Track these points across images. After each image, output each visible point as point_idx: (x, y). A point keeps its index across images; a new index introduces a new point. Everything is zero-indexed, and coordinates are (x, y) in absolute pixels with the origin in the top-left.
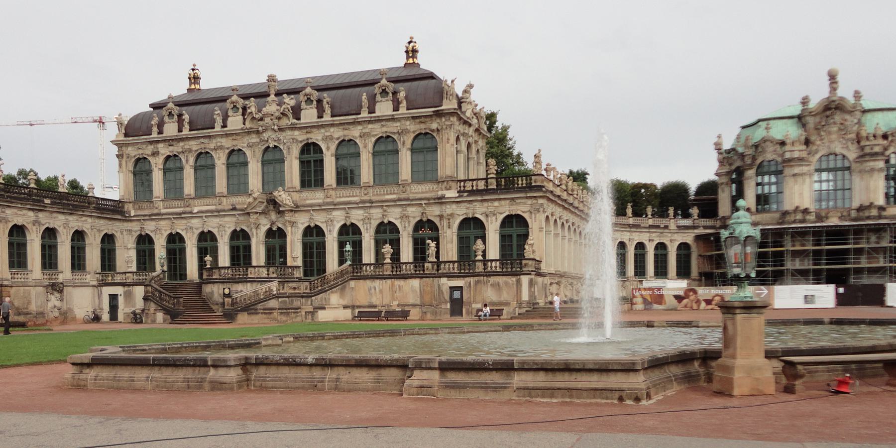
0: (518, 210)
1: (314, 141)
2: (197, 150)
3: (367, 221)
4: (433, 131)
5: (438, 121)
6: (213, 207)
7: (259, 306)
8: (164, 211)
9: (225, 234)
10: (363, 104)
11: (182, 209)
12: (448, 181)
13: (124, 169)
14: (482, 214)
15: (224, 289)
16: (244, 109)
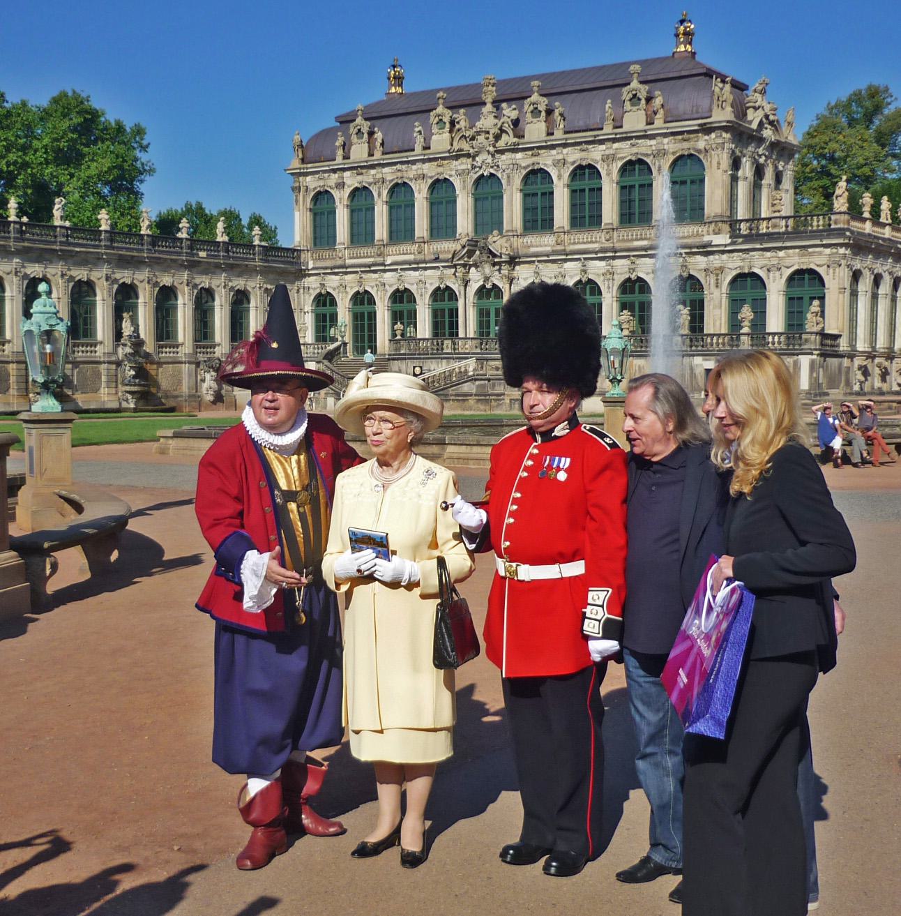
0: (810, 262)
1: (542, 167)
2: (392, 180)
3: (608, 276)
4: (699, 151)
5: (707, 137)
6: (411, 257)
7: (450, 391)
8: (349, 262)
9: (426, 292)
10: (607, 115)
11: (372, 260)
12: (717, 222)
13: (301, 207)
14: (761, 268)
15: (414, 367)
16: (453, 123)
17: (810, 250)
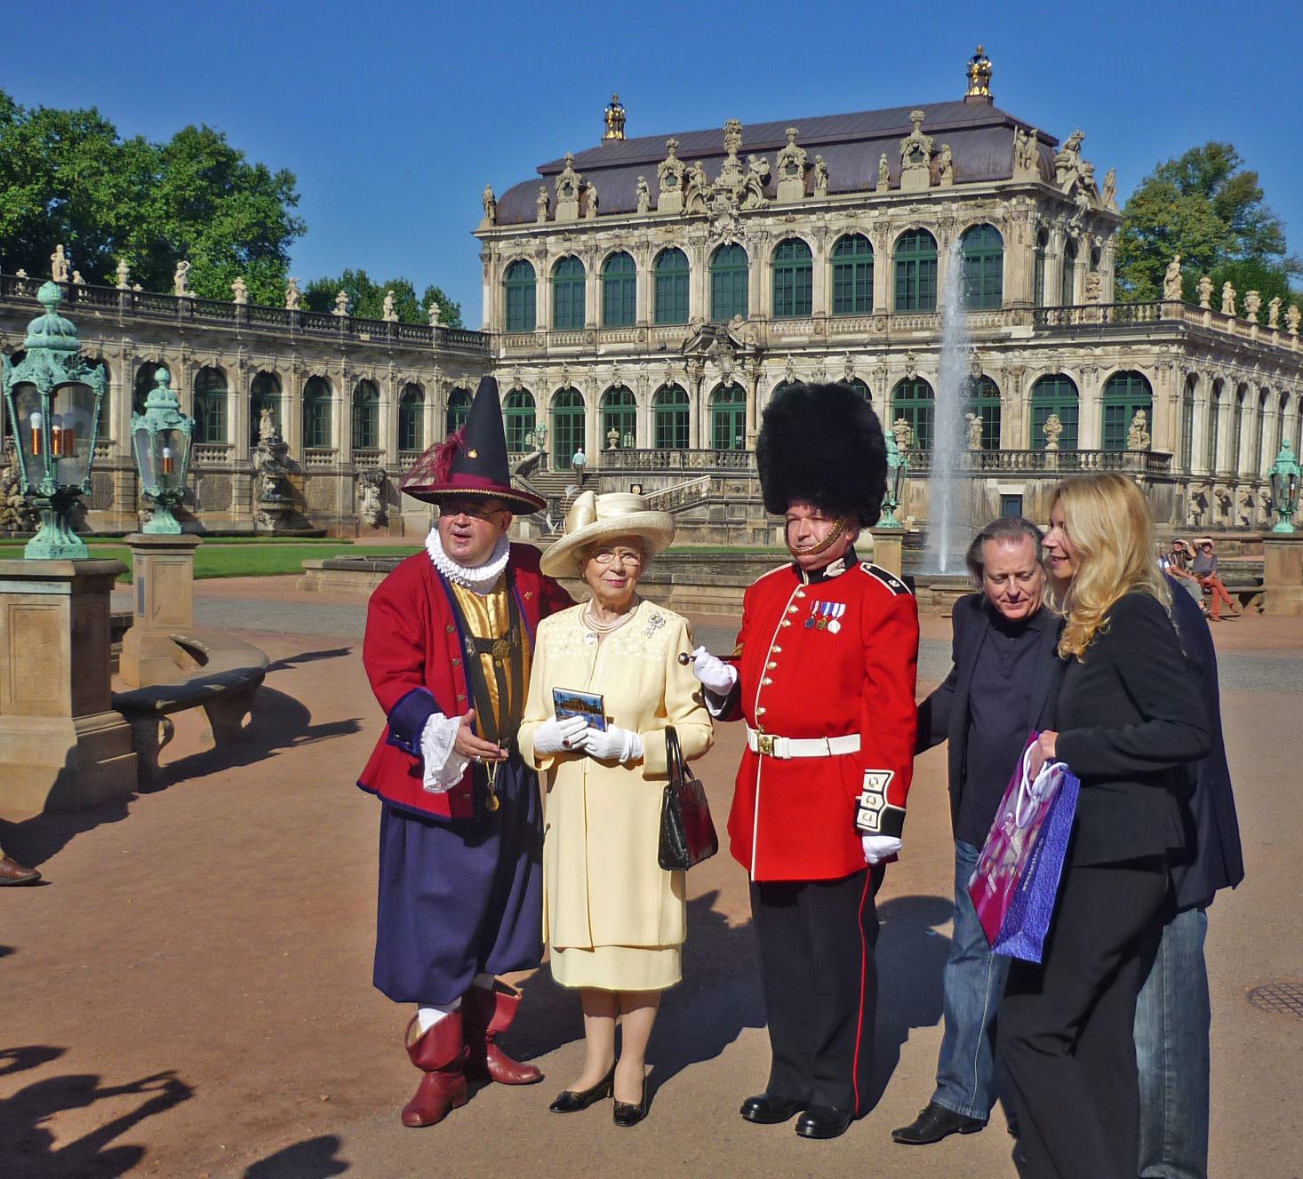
2: (608, 249)
3: (880, 376)
4: (996, 221)
5: (1006, 203)
6: (631, 346)
8: (551, 350)
10: (881, 172)
11: (580, 348)
15: (632, 486)
16: (686, 179)
17: (1134, 347)
